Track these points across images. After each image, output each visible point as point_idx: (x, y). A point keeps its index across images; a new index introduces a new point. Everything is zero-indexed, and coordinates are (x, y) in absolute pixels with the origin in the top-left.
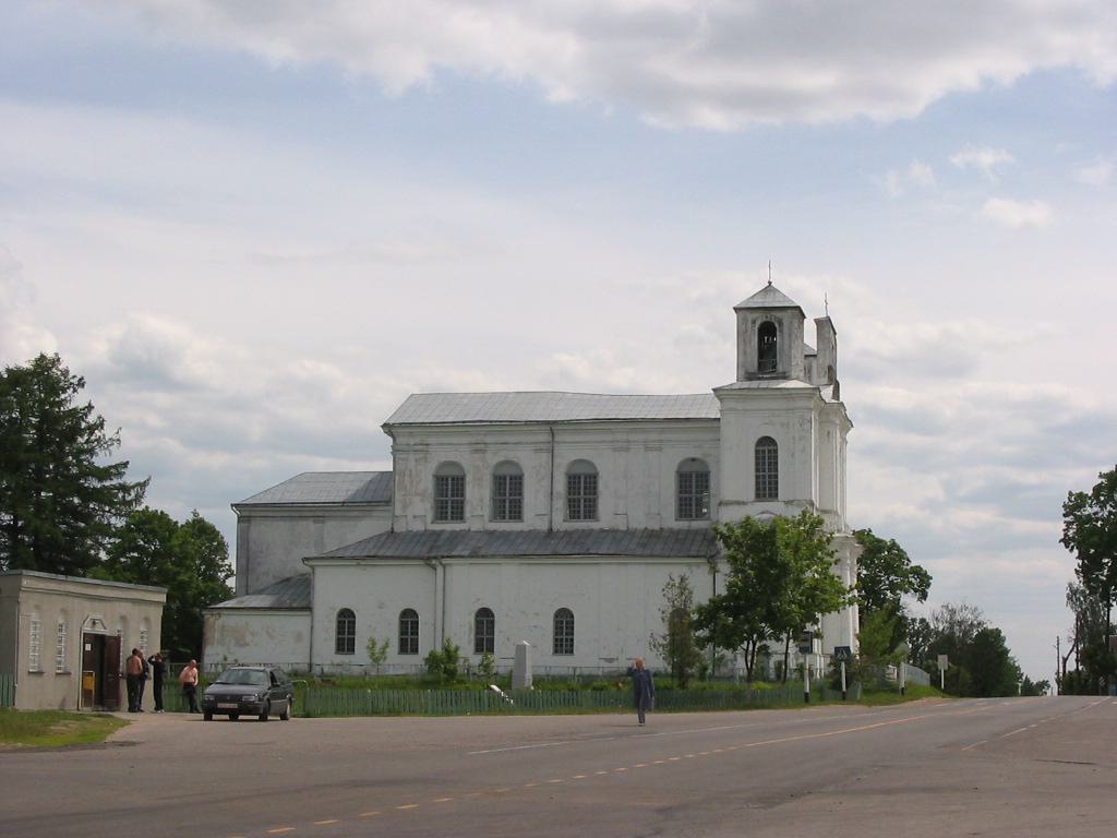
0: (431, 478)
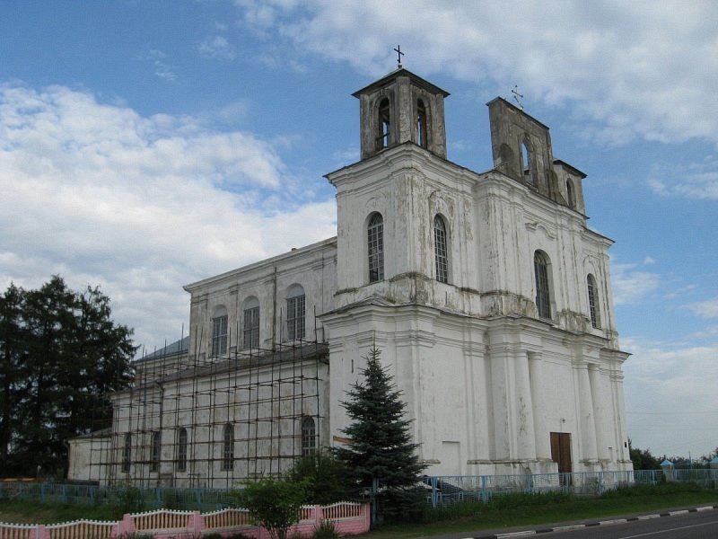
0: (208, 322)
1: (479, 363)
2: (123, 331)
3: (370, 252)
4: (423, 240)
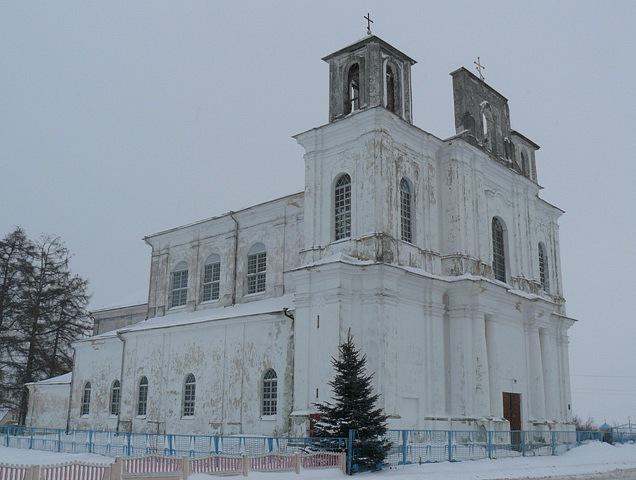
1: (438, 322)
2: (80, 284)
3: (337, 212)
4: (390, 202)
